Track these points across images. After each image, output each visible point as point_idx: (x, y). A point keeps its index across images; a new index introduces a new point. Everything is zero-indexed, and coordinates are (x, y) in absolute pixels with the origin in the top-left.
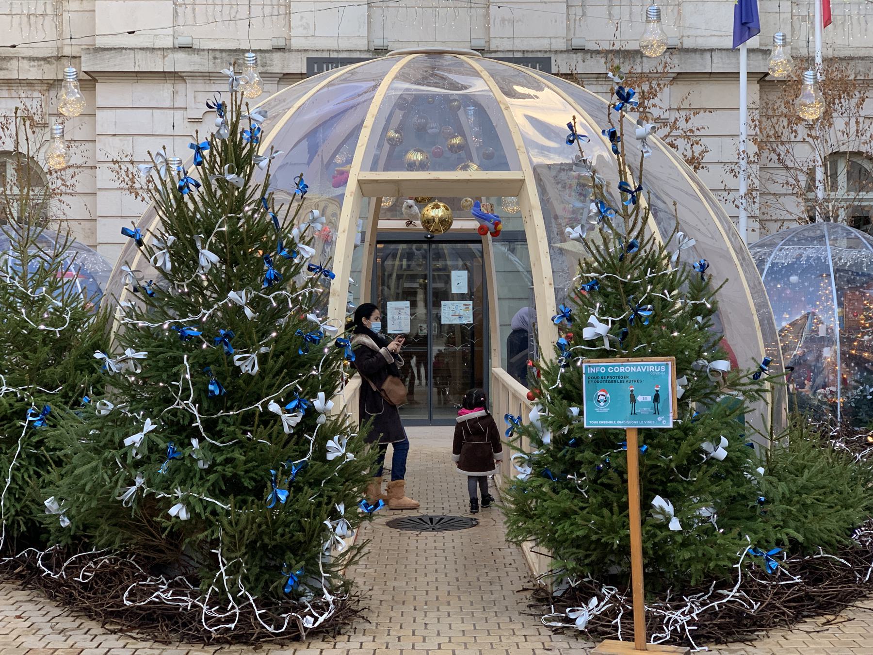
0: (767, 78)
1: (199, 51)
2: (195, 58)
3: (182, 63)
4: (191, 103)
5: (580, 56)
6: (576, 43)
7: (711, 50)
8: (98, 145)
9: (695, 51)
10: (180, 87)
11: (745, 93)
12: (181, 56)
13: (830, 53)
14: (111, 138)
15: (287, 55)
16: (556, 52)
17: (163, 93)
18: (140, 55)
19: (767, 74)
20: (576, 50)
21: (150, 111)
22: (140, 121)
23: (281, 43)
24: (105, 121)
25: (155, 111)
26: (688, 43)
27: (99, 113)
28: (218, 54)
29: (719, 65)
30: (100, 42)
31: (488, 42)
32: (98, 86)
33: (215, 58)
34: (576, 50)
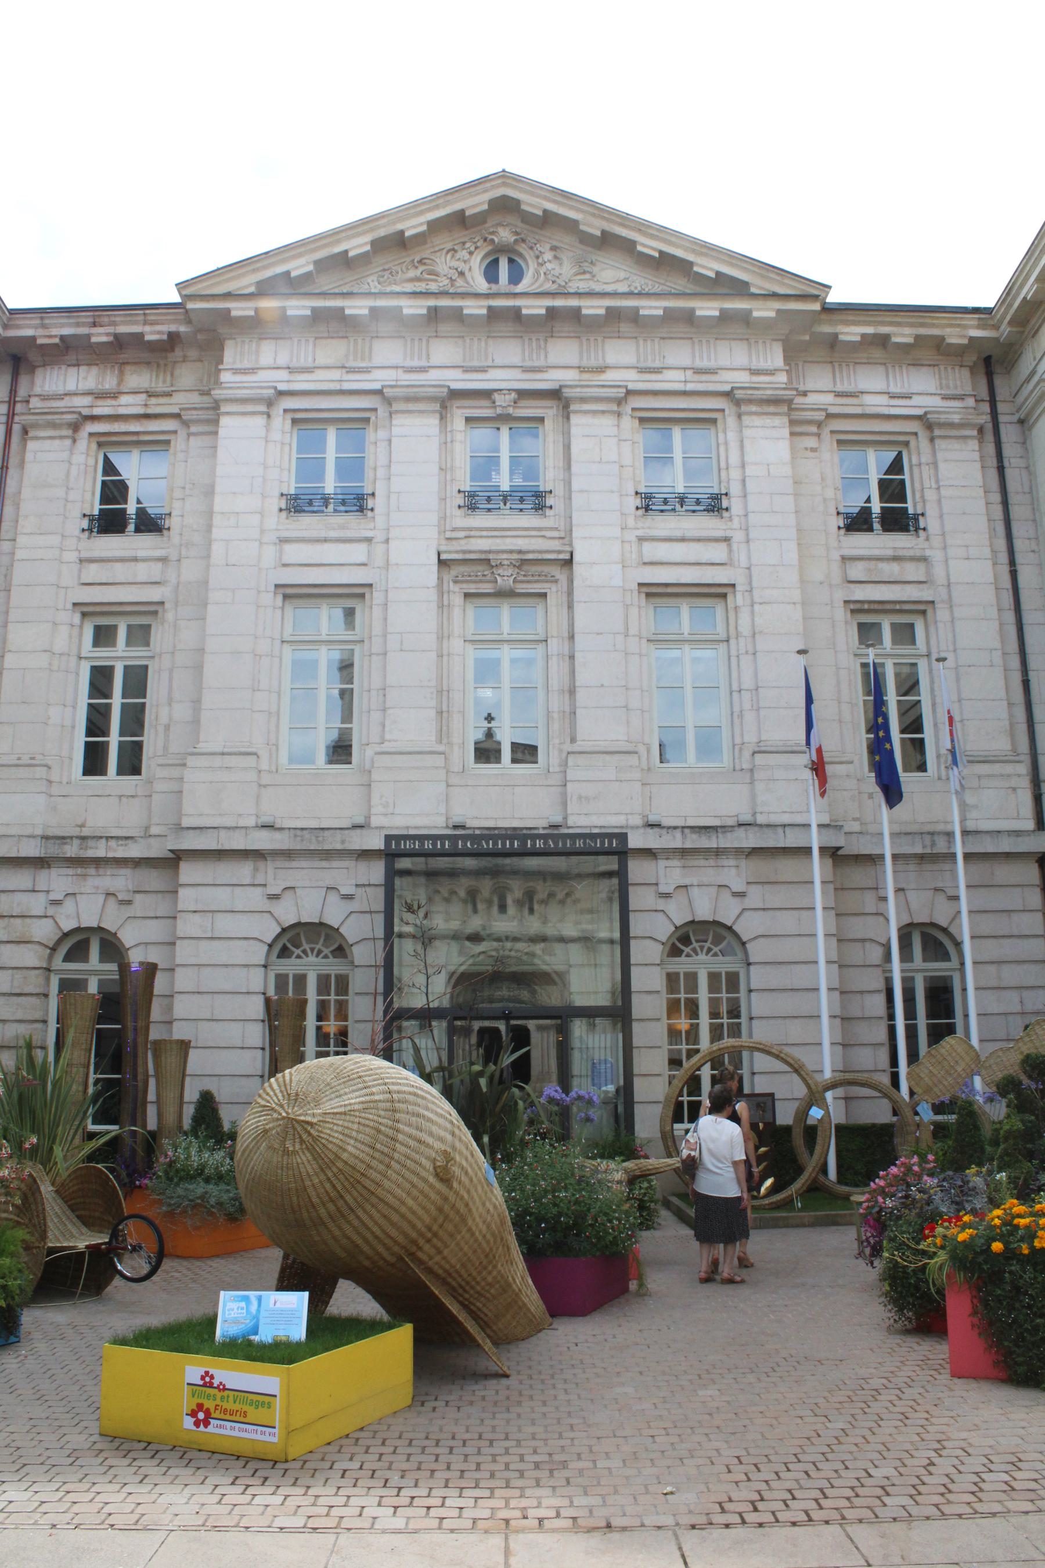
0: (840, 853)
1: (281, 829)
2: (277, 835)
3: (262, 841)
4: (270, 880)
5: (656, 830)
6: (653, 818)
7: (785, 826)
8: (178, 921)
9: (768, 826)
10: (261, 864)
11: (817, 867)
12: (265, 834)
13: (897, 829)
14: (191, 915)
15: (364, 831)
16: (632, 828)
17: (244, 871)
18: (223, 833)
19: (838, 848)
20: (652, 826)
21: (228, 889)
22: (221, 897)
23: (360, 820)
24: (186, 898)
25: (238, 890)
26: (761, 819)
27: (183, 892)
28: (299, 833)
29: (791, 840)
30: (186, 822)
31: (565, 818)
32: (184, 866)
33: (296, 836)
34: (652, 826)
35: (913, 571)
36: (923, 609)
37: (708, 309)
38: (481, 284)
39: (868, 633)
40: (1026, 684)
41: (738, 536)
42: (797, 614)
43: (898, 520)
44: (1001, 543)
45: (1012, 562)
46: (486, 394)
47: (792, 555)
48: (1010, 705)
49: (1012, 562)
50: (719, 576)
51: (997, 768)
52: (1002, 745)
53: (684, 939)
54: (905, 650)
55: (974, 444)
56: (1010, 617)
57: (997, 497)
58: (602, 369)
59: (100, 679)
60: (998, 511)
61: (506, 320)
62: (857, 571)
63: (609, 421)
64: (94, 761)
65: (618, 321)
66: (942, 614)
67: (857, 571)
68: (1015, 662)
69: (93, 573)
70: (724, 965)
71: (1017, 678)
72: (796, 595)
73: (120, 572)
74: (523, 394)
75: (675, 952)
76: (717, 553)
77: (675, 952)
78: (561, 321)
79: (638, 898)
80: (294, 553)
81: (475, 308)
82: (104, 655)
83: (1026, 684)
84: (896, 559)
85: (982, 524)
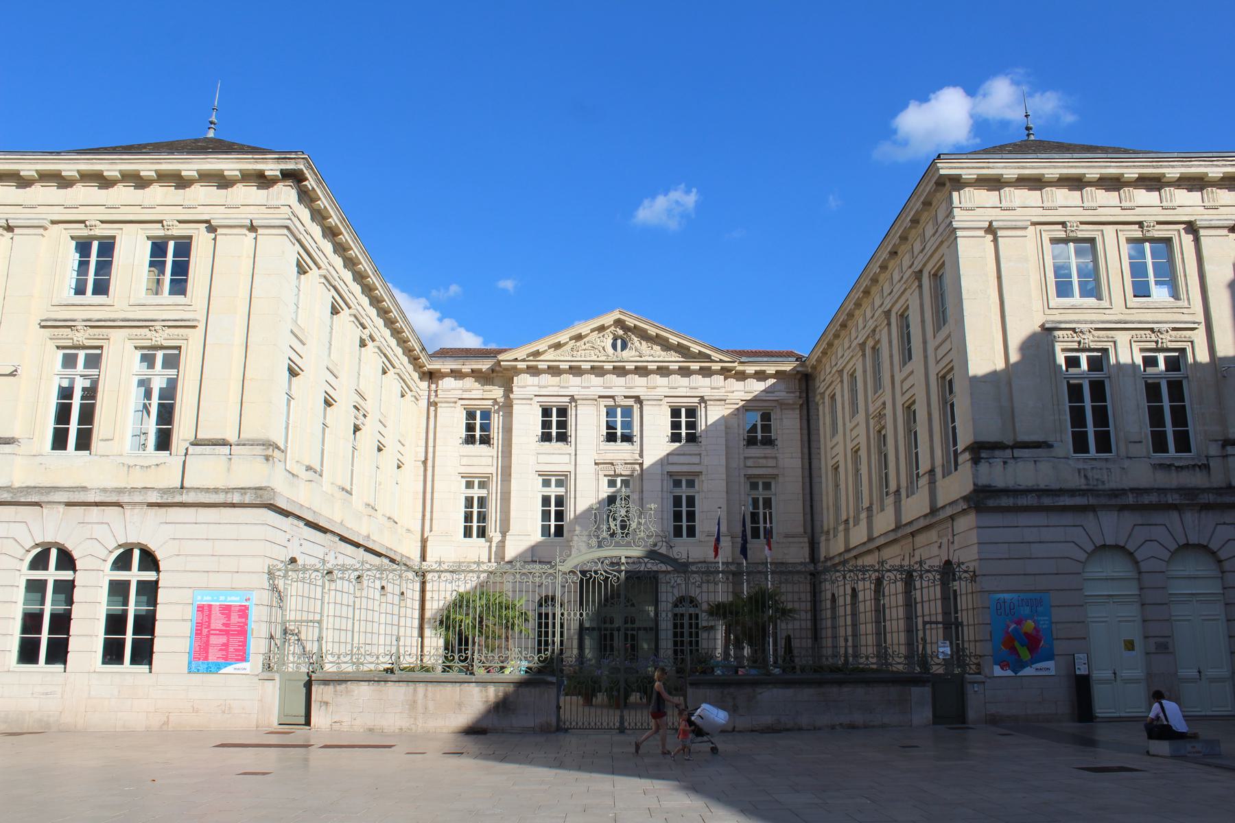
35: (771, 463)
36: (775, 477)
37: (695, 366)
38: (610, 350)
39: (754, 486)
40: (812, 506)
41: (704, 453)
42: (724, 484)
43: (768, 442)
44: (806, 451)
45: (810, 459)
46: (613, 397)
47: (723, 462)
48: (804, 514)
49: (810, 459)
50: (697, 469)
51: (796, 540)
52: (801, 530)
53: (680, 601)
54: (767, 492)
55: (798, 412)
56: (807, 480)
57: (805, 432)
58: (654, 388)
59: (469, 502)
60: (806, 438)
61: (620, 371)
62: (749, 463)
63: (657, 408)
64: (468, 533)
65: (663, 371)
66: (781, 479)
67: (749, 463)
68: (808, 497)
69: (465, 461)
70: (692, 610)
71: (808, 503)
72: (724, 476)
73: (475, 461)
74: (626, 397)
75: (676, 606)
76: (696, 460)
77: (676, 606)
78: (642, 371)
79: (662, 588)
80: (542, 459)
81: (609, 366)
82: (470, 493)
83: (812, 506)
84: (765, 458)
85: (799, 443)
